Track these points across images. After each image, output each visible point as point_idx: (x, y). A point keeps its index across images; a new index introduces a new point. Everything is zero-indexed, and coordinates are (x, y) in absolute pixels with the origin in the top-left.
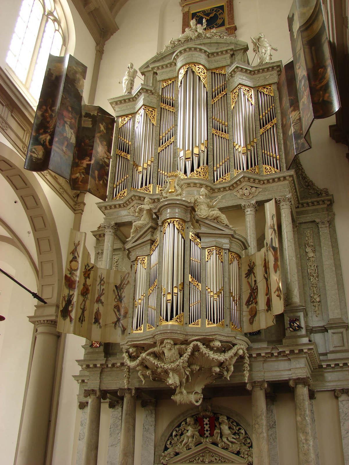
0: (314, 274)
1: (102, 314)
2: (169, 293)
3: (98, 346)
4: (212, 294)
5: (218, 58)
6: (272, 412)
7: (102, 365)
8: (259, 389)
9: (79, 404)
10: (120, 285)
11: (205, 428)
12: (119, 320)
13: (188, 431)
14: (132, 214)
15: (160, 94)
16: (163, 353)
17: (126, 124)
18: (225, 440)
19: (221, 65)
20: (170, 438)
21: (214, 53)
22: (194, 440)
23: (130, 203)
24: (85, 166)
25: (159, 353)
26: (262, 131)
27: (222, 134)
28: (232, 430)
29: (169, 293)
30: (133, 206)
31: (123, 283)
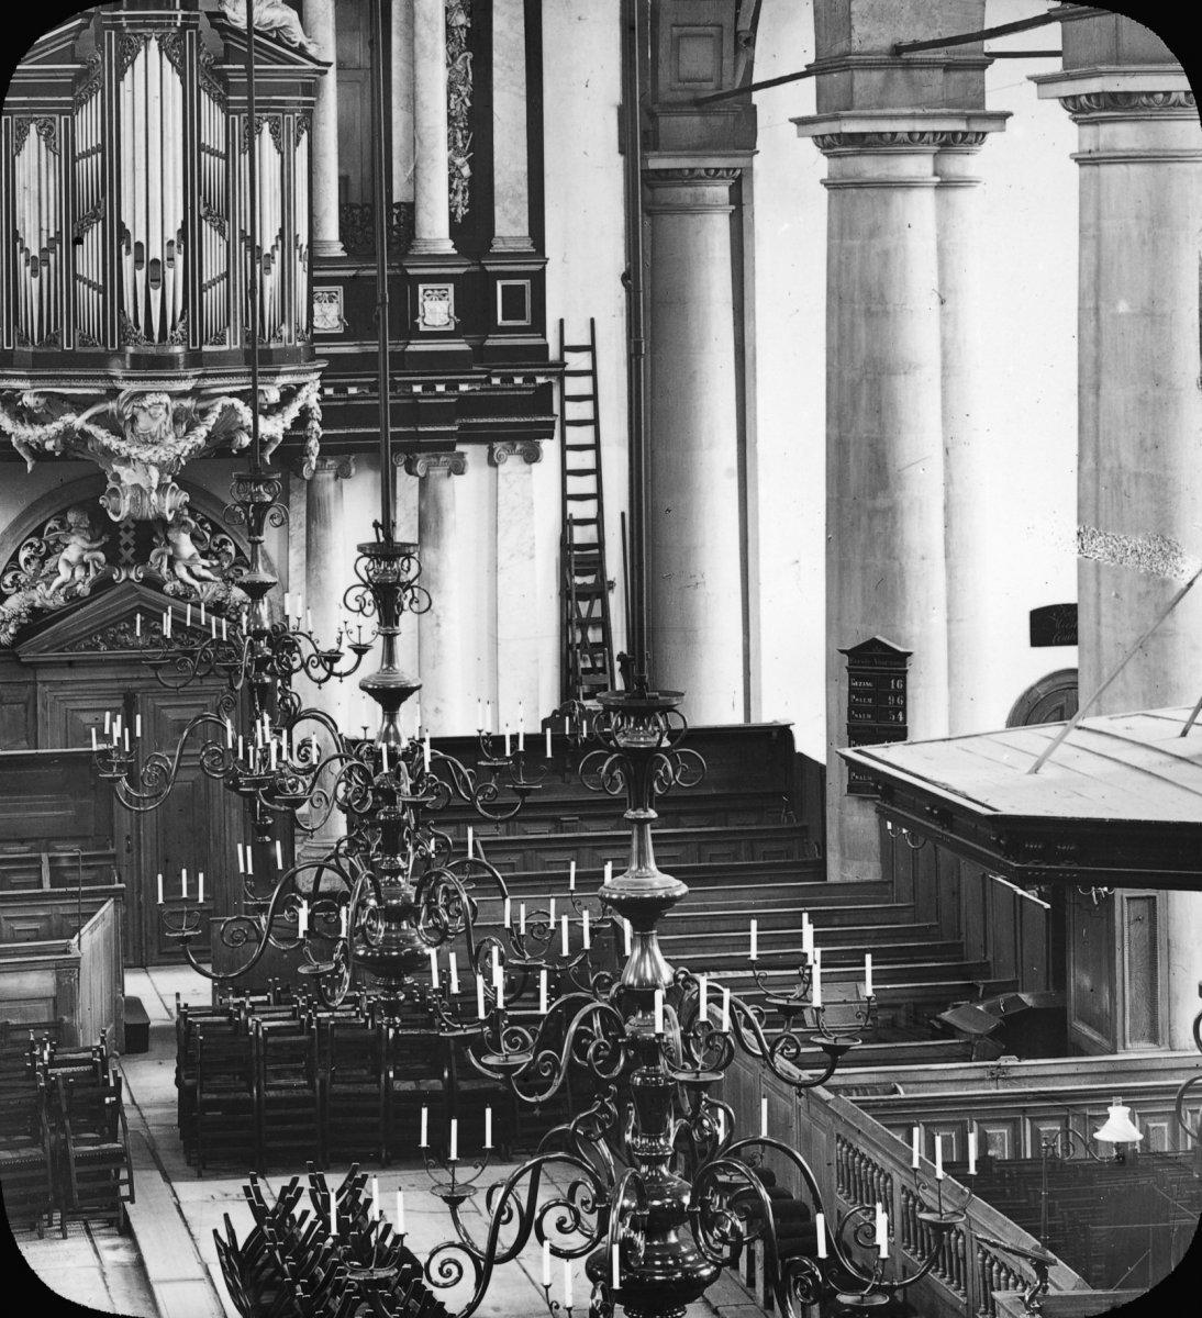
0: (461, 88)
13: (66, 546)
16: (134, 419)
18: (182, 572)
22: (92, 574)
25: (121, 415)
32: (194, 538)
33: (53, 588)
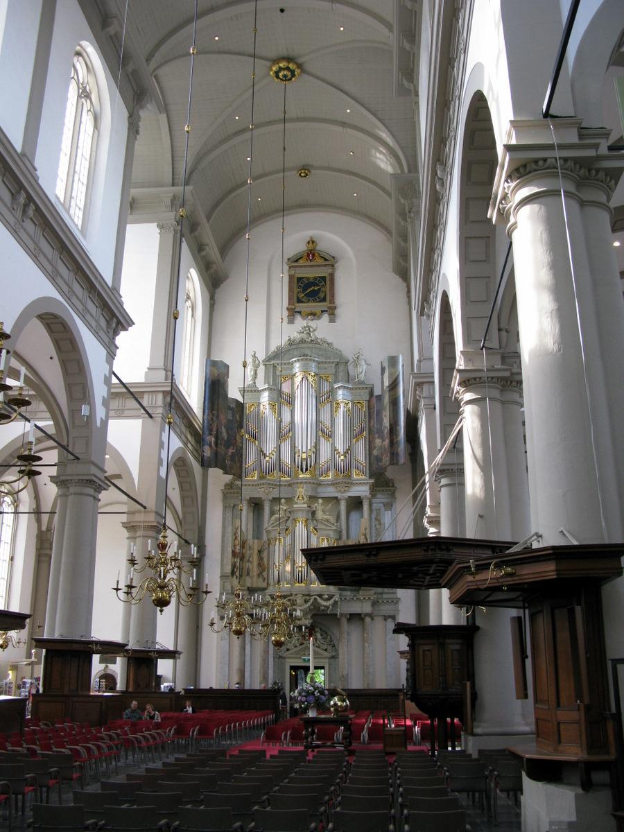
12: (261, 573)
18: (318, 642)
24: (230, 454)
32: (321, 635)
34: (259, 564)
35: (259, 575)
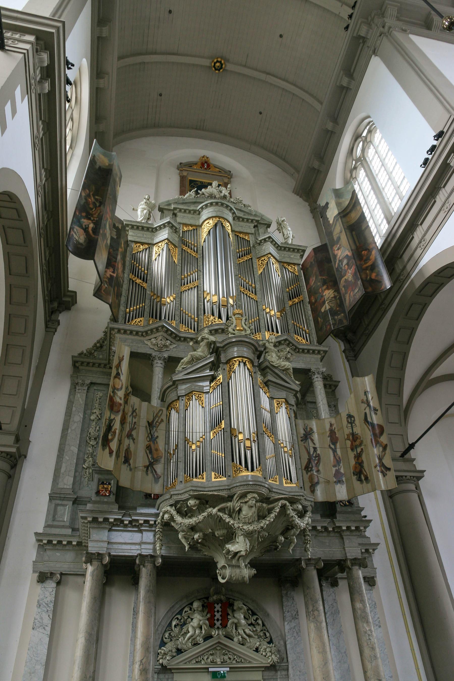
1: (133, 453)
2: (248, 439)
3: (107, 495)
4: (286, 449)
5: (242, 224)
6: (293, 599)
7: (115, 519)
8: (313, 567)
9: (37, 575)
10: (153, 421)
11: (215, 616)
13: (192, 619)
14: (151, 347)
15: (181, 236)
16: (240, 510)
17: (140, 251)
18: (241, 632)
19: (245, 231)
20: (168, 629)
21: (241, 217)
22: (203, 632)
23: (152, 334)
25: (234, 510)
26: (290, 303)
27: (250, 294)
28: (247, 621)
29: (248, 439)
30: (155, 338)
31: (156, 420)
32: (245, 618)
33: (186, 639)
34: (148, 447)
35: (147, 467)
